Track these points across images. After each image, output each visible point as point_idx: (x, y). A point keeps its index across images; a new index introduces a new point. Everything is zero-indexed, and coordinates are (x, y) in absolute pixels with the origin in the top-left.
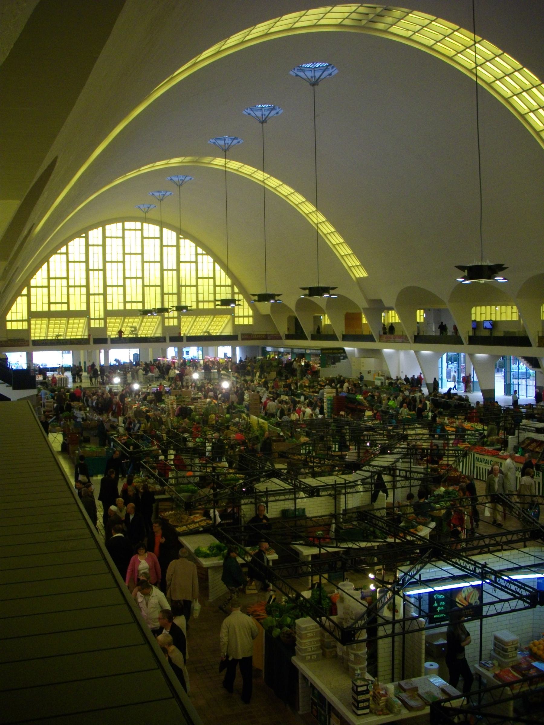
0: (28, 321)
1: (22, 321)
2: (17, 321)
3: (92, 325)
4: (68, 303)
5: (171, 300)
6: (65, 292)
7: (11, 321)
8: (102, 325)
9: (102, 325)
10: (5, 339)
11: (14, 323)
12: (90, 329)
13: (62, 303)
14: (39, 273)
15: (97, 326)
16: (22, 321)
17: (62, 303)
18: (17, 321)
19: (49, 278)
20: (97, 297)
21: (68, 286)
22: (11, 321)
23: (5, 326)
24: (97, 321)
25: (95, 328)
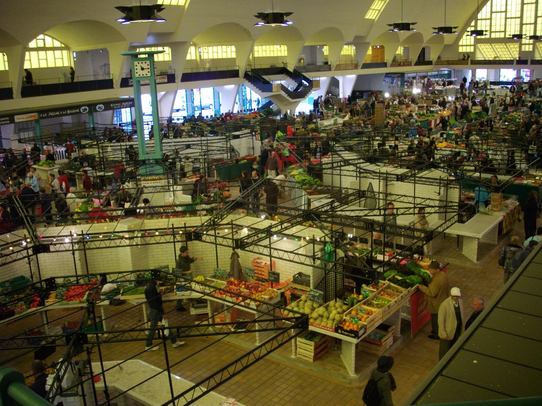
0: (475, 46)
1: (470, 45)
2: (466, 46)
3: (523, 49)
4: (505, 32)
5: (528, 29)
6: (503, 23)
7: (462, 46)
8: (531, 50)
9: (531, 50)
10: (457, 59)
11: (464, 47)
12: (521, 52)
13: (500, 32)
14: (484, 9)
15: (527, 50)
16: (470, 45)
17: (500, 32)
18: (466, 46)
19: (492, 12)
20: (528, 26)
21: (506, 18)
22: (462, 46)
23: (458, 49)
24: (527, 46)
25: (525, 52)
